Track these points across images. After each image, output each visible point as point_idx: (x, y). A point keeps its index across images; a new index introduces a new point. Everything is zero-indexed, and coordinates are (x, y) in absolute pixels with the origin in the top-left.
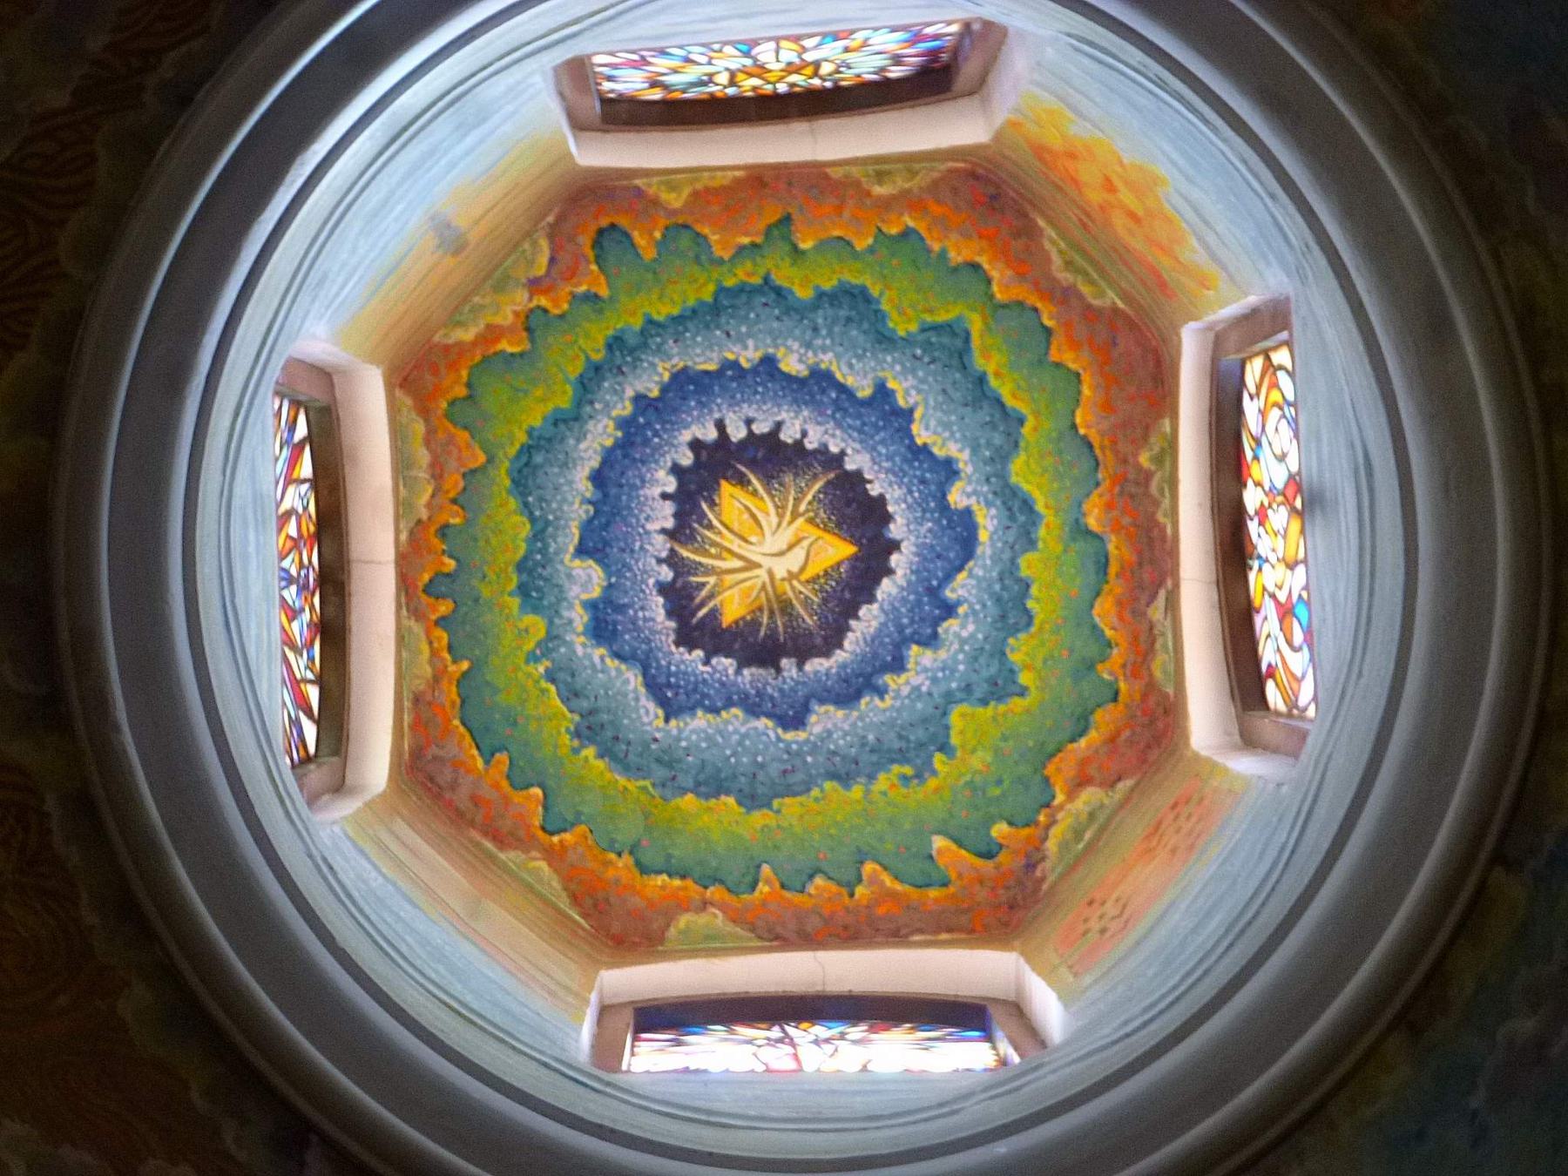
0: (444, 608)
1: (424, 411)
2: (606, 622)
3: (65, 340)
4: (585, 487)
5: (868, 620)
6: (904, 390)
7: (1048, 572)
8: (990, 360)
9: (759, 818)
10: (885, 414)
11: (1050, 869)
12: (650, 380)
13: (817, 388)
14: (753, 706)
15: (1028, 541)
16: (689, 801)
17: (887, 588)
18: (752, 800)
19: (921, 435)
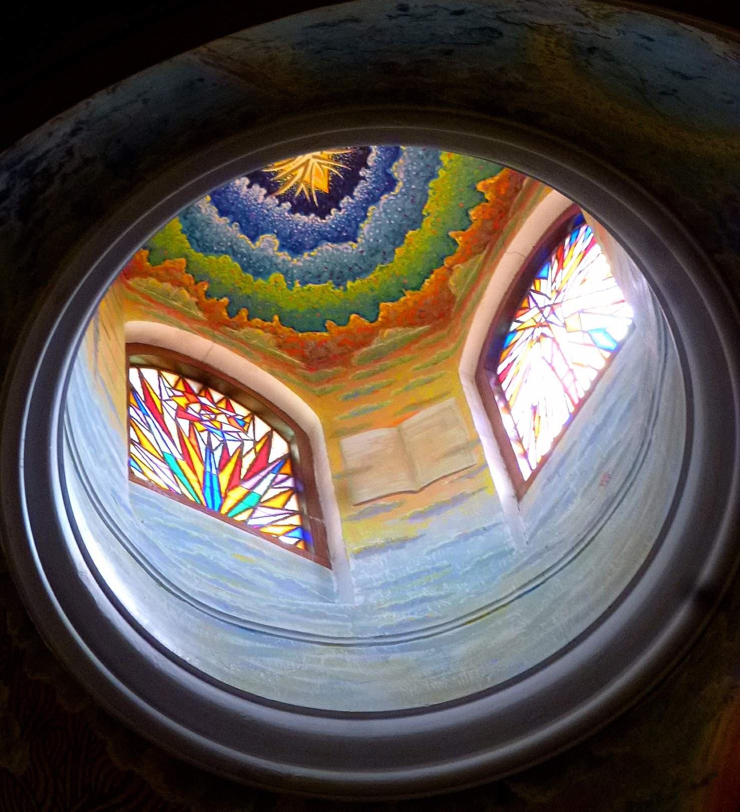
0: (244, 313)
1: (146, 274)
2: (294, 244)
4: (225, 220)
9: (426, 224)
14: (372, 198)
18: (416, 224)
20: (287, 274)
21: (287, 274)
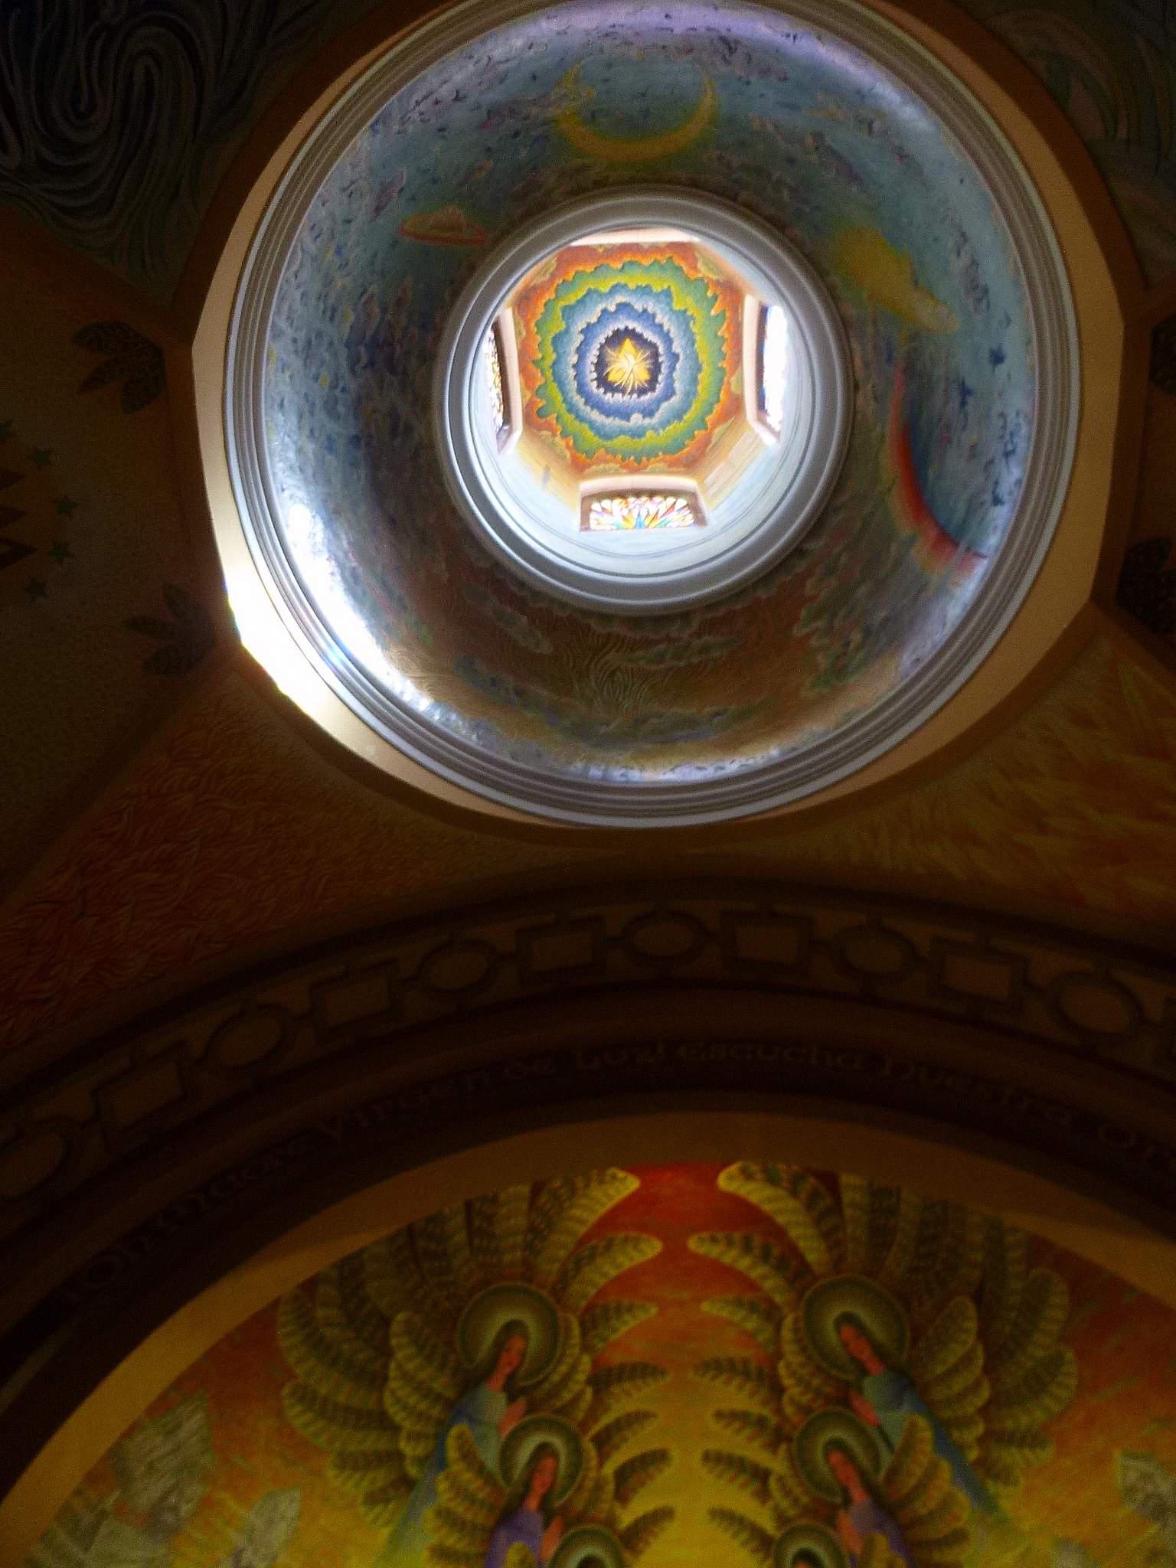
1: (589, 466)
2: (648, 412)
3: (587, 613)
4: (610, 420)
5: (649, 335)
6: (582, 325)
7: (635, 279)
8: (572, 299)
9: (705, 367)
10: (589, 331)
11: (721, 279)
12: (579, 401)
13: (581, 351)
14: (672, 368)
15: (625, 286)
16: (699, 388)
17: (639, 330)
18: (699, 369)
19: (594, 320)
20: (655, 429)
21: (655, 429)
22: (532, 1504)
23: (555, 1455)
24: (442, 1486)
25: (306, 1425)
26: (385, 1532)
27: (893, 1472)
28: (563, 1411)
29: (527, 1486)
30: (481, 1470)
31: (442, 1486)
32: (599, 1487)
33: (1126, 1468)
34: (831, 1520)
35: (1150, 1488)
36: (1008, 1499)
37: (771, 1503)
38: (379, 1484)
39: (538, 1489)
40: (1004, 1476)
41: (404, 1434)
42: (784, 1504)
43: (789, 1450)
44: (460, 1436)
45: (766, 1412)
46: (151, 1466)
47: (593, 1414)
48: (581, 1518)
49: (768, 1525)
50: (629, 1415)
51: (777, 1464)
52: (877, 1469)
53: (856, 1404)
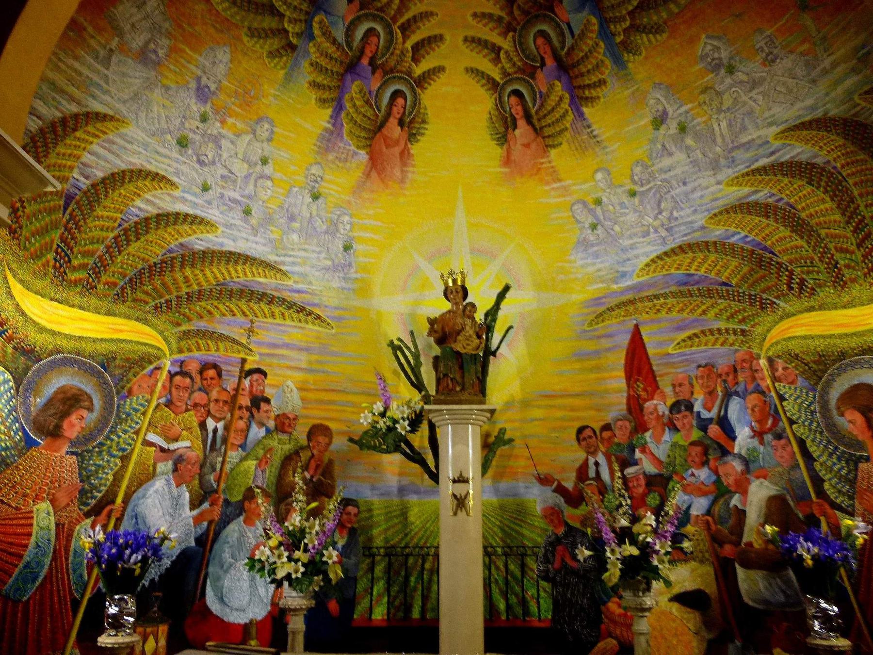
22: (365, 61)
23: (379, 37)
24: (312, 50)
25: (224, 10)
26: (282, 72)
27: (572, 48)
28: (381, 9)
29: (362, 52)
30: (335, 41)
31: (312, 50)
32: (403, 53)
33: (705, 43)
34: (533, 77)
35: (716, 55)
36: (634, 63)
37: (500, 65)
38: (275, 47)
39: (368, 53)
40: (634, 50)
41: (286, 19)
42: (507, 66)
43: (513, 37)
44: (320, 22)
45: (503, 14)
46: (133, 26)
47: (400, 11)
48: (392, 71)
49: (497, 76)
50: (421, 14)
51: (506, 44)
52: (562, 48)
53: (556, 9)
